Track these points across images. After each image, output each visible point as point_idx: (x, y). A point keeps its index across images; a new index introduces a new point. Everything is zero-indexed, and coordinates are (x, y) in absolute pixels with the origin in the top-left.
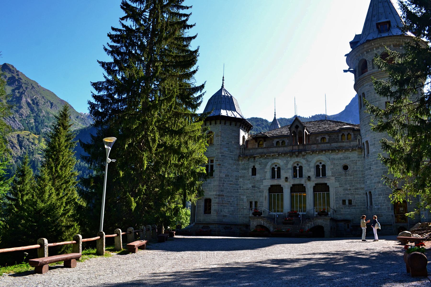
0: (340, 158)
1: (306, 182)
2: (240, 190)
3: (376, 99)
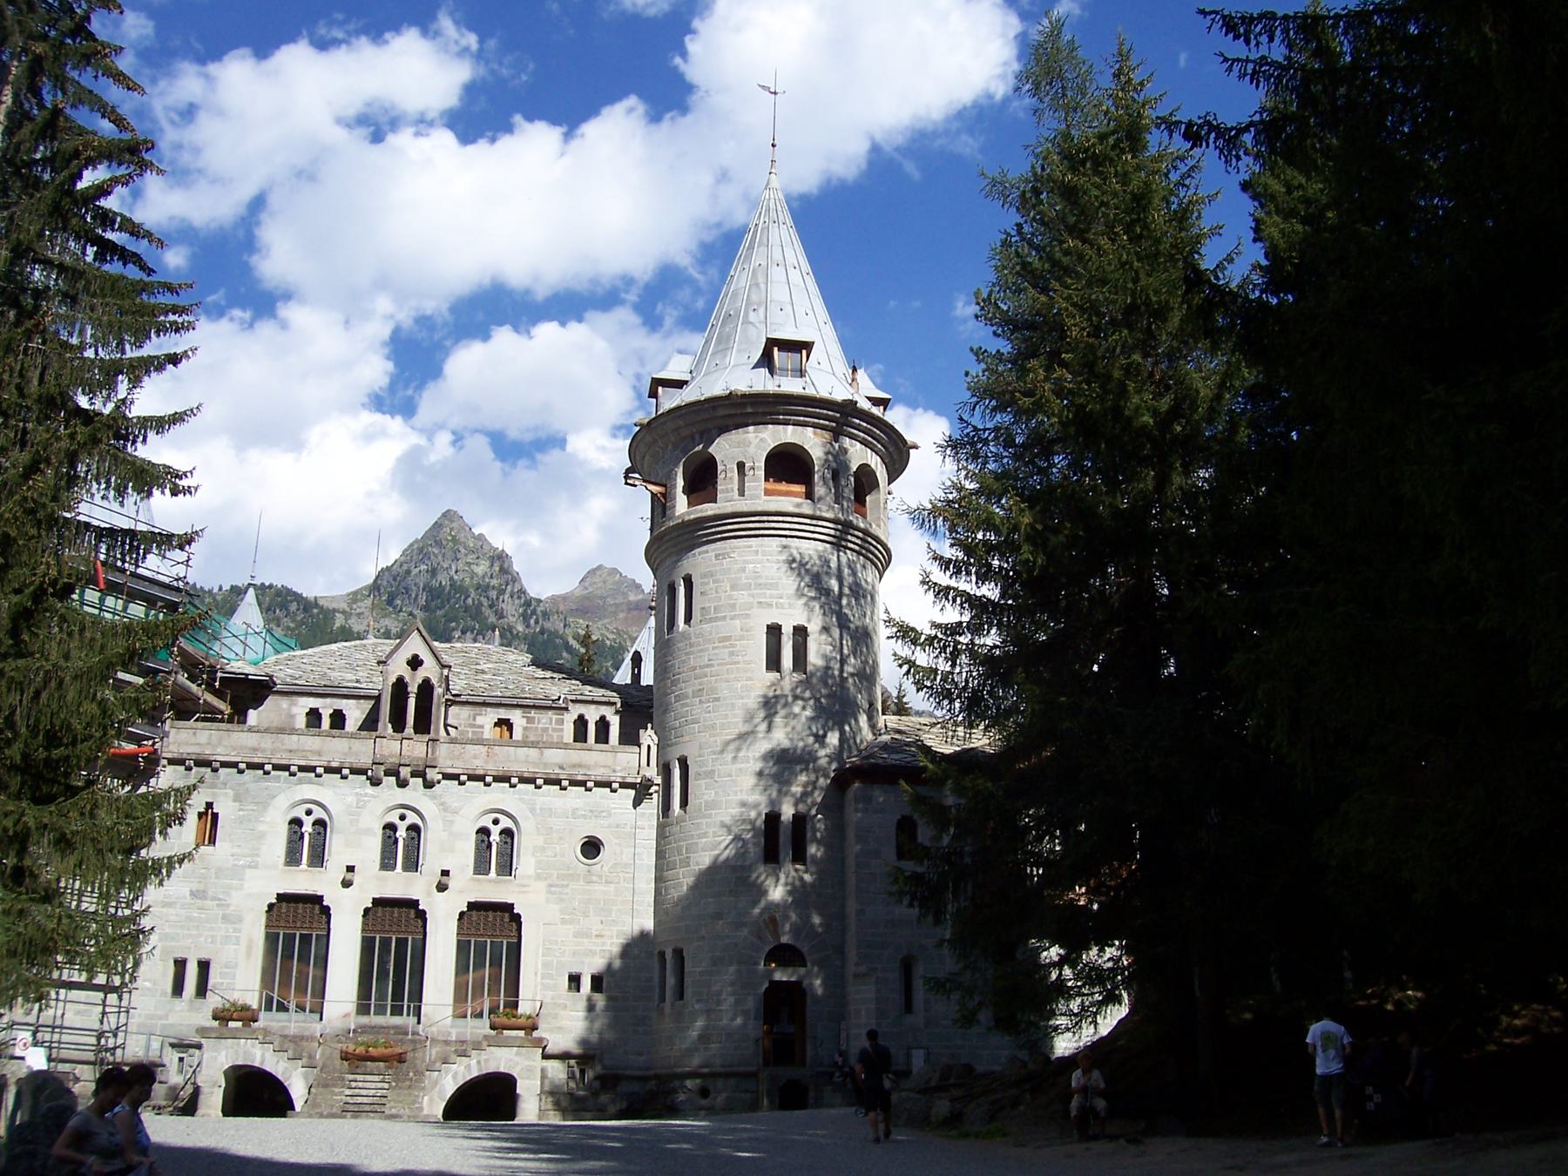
0: (575, 810)
1: (429, 894)
3: (733, 606)
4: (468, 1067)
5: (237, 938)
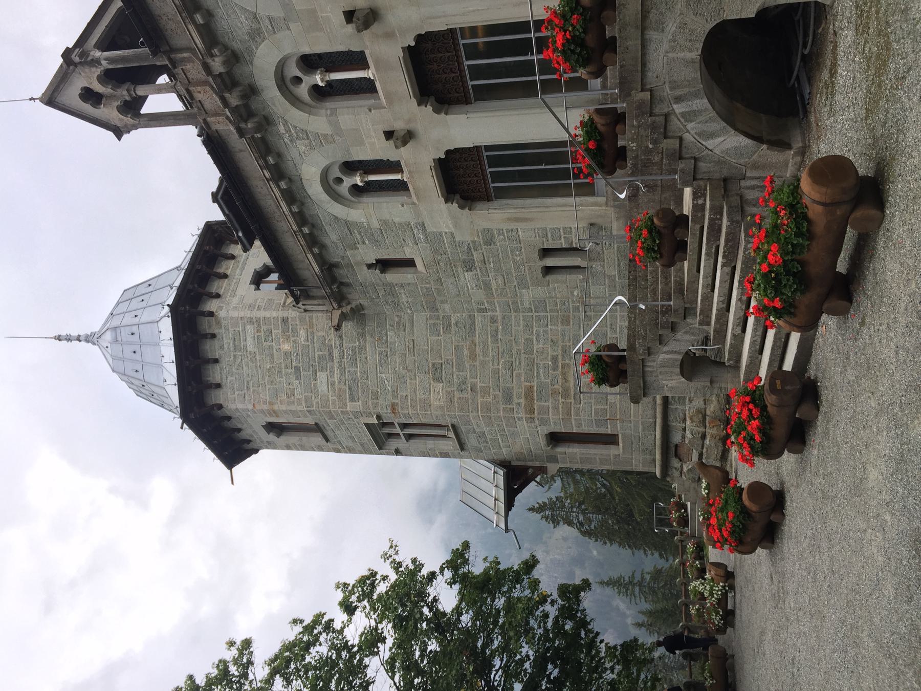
4: (689, 116)
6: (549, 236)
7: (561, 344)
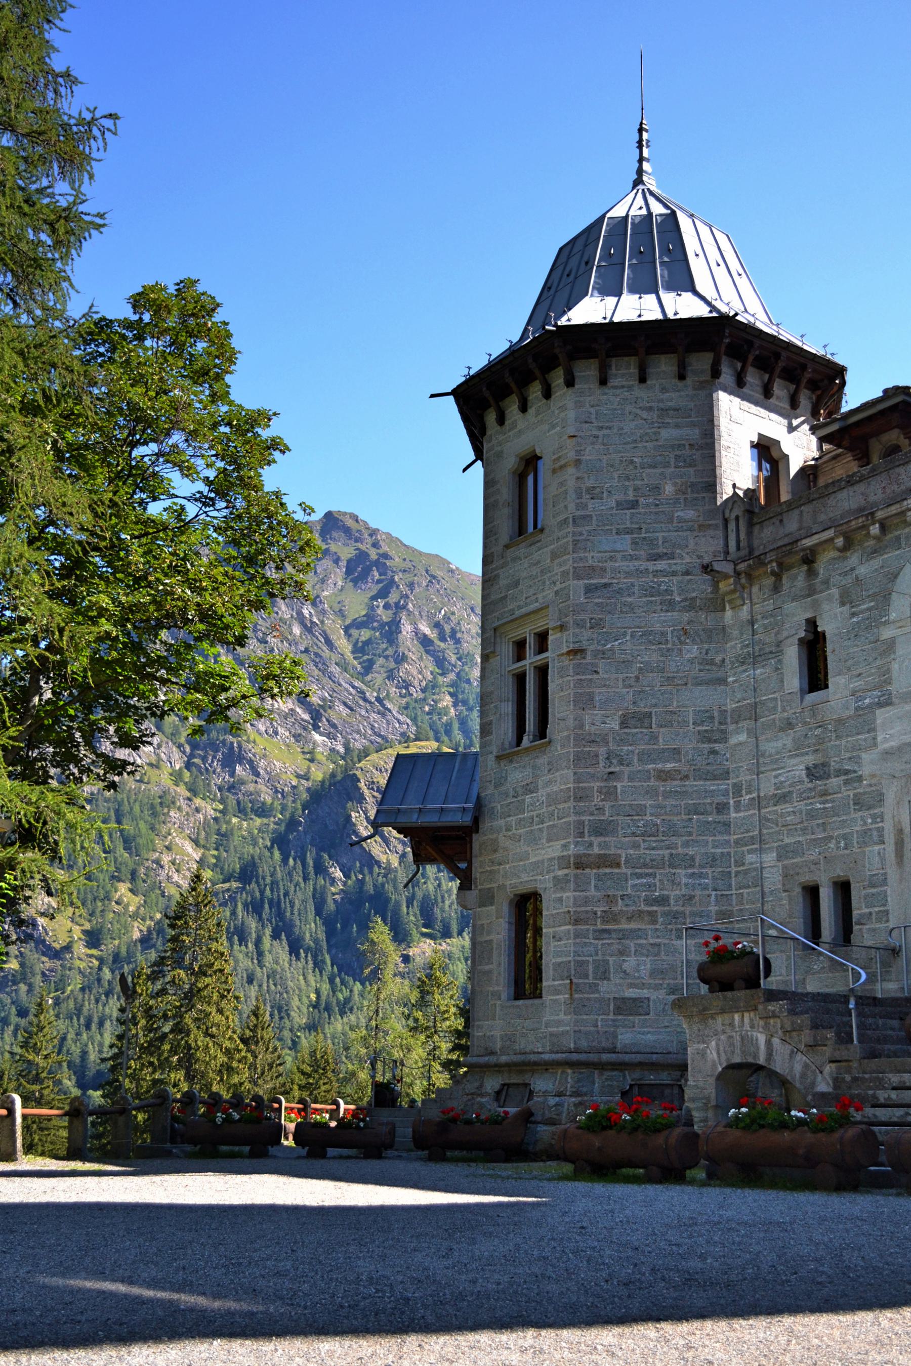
2: (737, 809)
5: (880, 830)
6: (873, 890)
7: (688, 909)
